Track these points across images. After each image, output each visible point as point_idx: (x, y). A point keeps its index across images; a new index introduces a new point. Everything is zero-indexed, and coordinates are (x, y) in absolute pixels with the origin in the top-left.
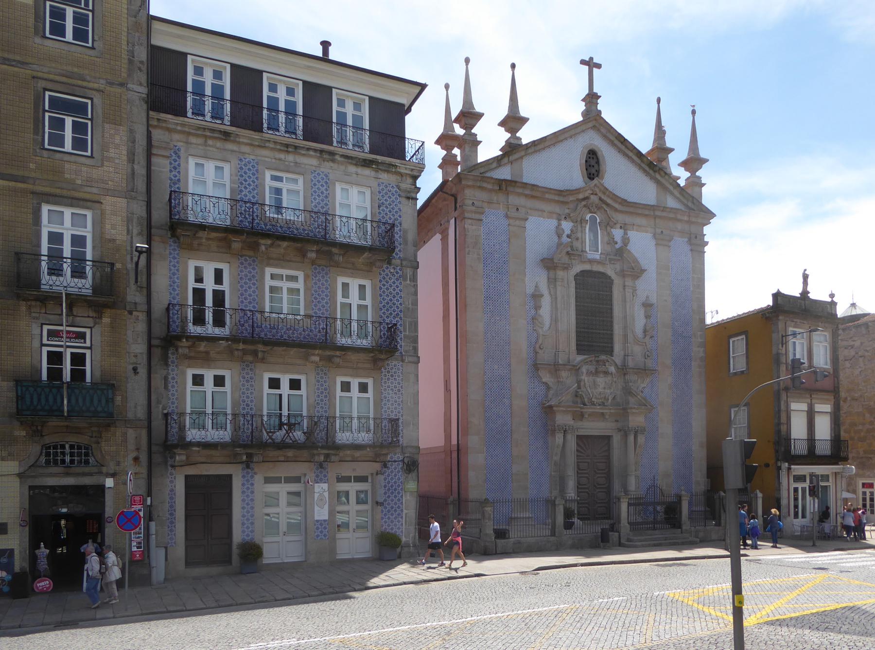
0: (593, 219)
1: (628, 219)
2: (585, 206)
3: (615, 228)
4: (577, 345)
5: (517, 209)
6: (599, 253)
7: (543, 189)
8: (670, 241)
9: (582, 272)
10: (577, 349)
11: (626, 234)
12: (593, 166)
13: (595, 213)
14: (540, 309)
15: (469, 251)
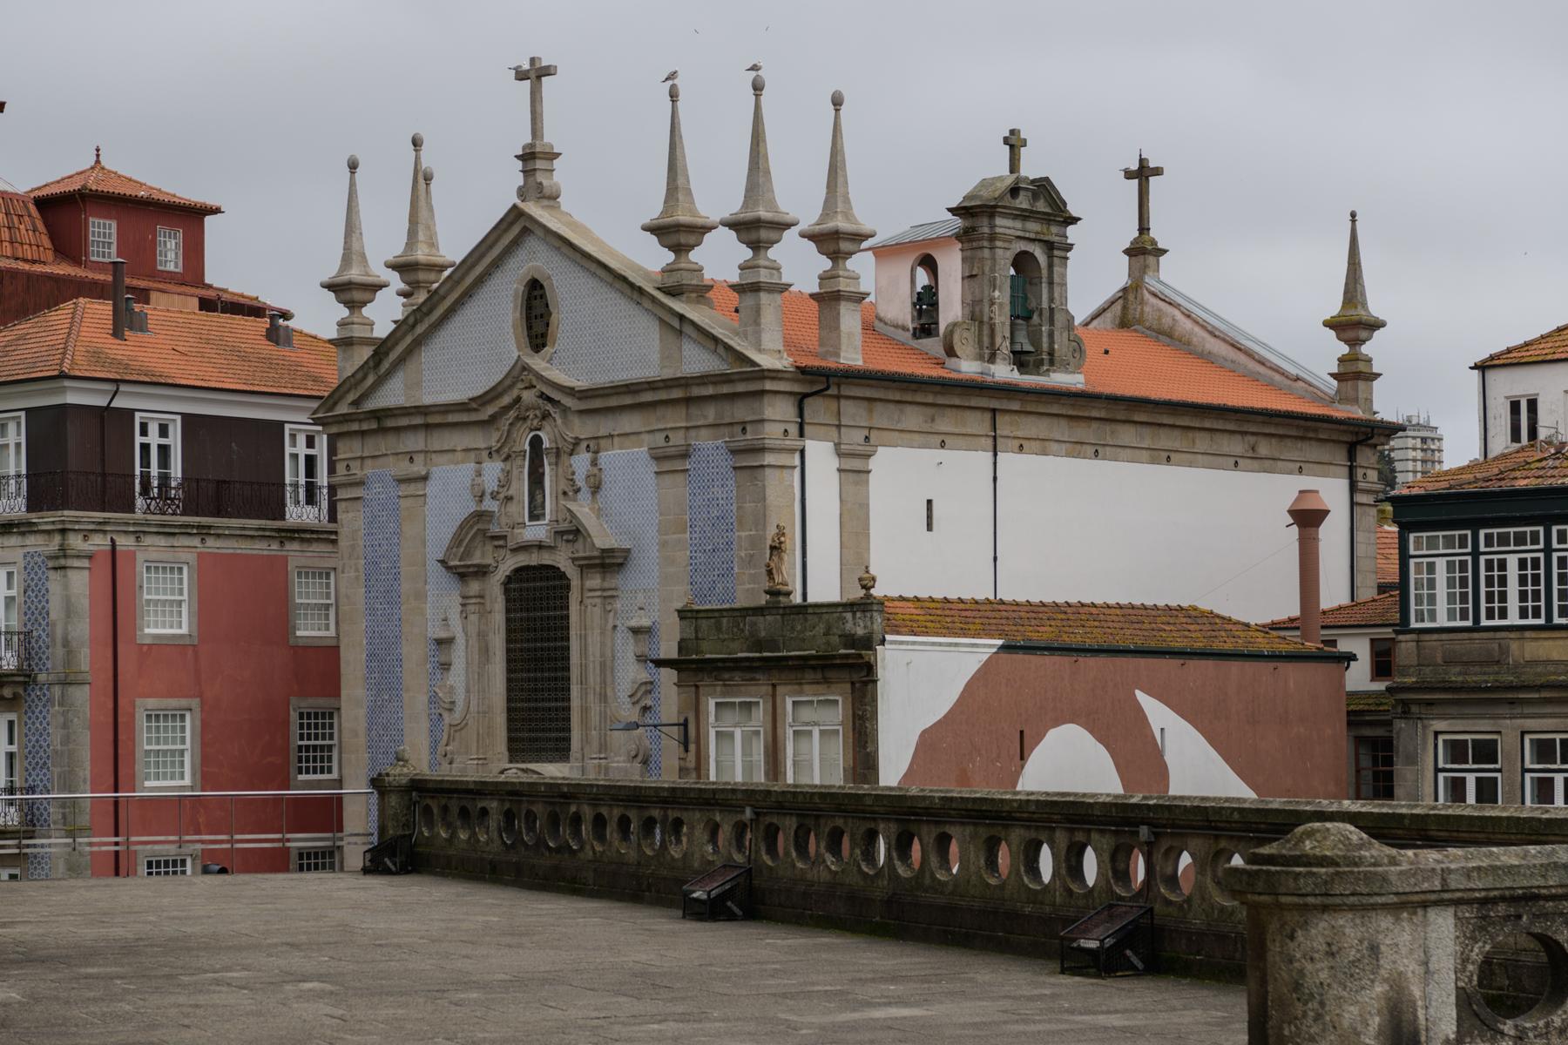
0: (536, 443)
1: (604, 426)
2: (517, 418)
3: (578, 454)
4: (510, 740)
5: (411, 458)
6: (546, 522)
7: (437, 409)
8: (685, 455)
9: (518, 570)
10: (510, 750)
11: (594, 463)
12: (542, 316)
13: (539, 430)
14: (448, 669)
15: (344, 564)
